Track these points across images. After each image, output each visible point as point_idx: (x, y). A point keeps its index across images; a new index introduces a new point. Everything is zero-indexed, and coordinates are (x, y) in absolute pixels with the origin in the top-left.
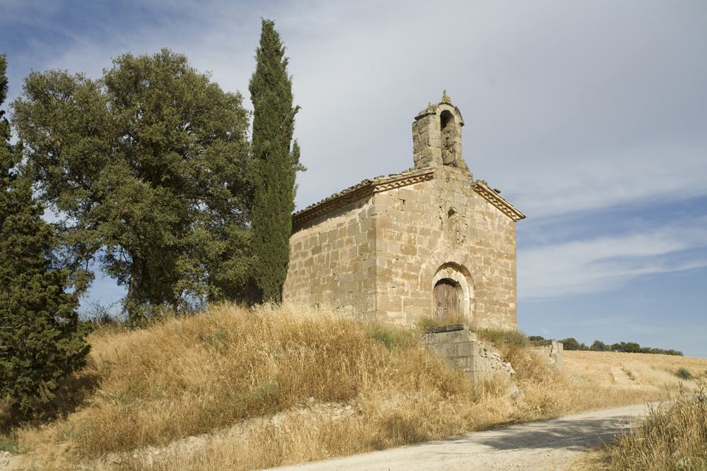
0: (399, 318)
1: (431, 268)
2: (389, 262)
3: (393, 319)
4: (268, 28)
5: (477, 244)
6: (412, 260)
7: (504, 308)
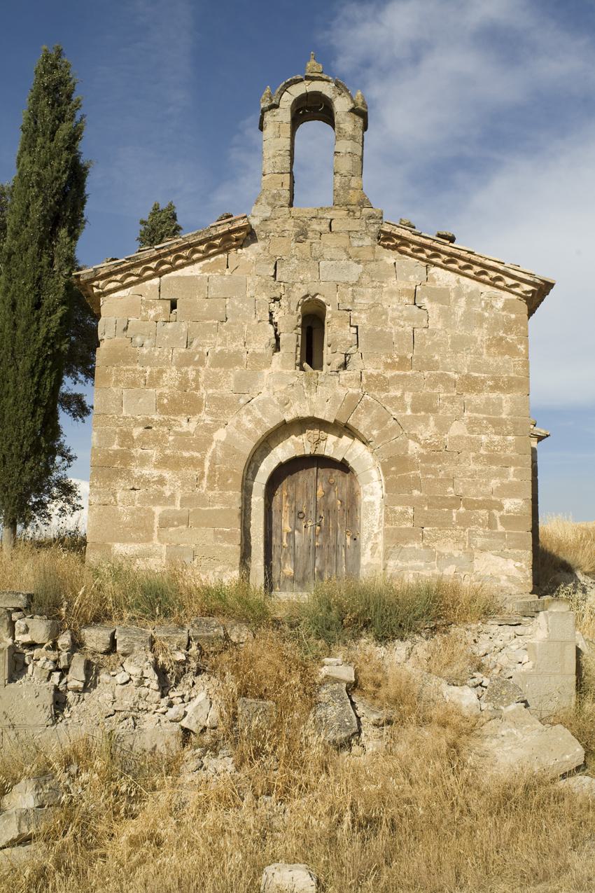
0: (145, 555)
1: (241, 437)
2: (126, 436)
3: (131, 559)
4: (52, 64)
5: (388, 366)
6: (186, 425)
7: (483, 512)
